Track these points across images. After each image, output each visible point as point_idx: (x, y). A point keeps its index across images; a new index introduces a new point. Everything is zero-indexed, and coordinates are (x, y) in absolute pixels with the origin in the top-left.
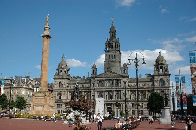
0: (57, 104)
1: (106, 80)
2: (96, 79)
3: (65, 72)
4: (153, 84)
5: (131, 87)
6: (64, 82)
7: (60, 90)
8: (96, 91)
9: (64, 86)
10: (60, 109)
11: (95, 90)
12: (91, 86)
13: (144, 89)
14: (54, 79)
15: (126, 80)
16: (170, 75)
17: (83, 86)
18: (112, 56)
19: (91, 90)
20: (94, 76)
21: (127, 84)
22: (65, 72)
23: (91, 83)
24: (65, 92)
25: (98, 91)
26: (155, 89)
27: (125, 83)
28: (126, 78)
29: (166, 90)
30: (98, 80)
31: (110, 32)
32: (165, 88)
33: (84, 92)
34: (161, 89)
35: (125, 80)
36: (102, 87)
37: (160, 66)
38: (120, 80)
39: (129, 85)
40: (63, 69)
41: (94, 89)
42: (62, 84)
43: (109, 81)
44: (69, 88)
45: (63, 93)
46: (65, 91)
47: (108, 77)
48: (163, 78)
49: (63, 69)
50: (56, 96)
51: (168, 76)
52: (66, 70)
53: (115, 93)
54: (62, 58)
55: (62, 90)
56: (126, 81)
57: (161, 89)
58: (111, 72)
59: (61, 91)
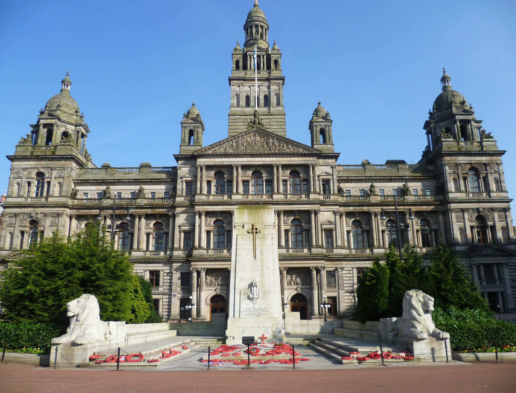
1: (245, 167)
2: (201, 161)
3: (65, 134)
4: (441, 190)
5: (351, 200)
6: (55, 173)
9: (55, 190)
11: (197, 208)
14: (12, 159)
15: (329, 170)
16: (501, 153)
20: (190, 150)
21: (334, 186)
22: (65, 134)
24: (58, 215)
25: (208, 214)
26: (453, 206)
27: (326, 183)
28: (330, 161)
29: (492, 210)
30: (209, 168)
32: (489, 205)
33: (143, 220)
34: (475, 206)
35: (322, 169)
37: (461, 121)
38: (306, 167)
39: (340, 190)
40: (60, 120)
42: (49, 183)
43: (257, 170)
44: (76, 202)
47: (253, 155)
48: (475, 166)
49: (60, 120)
52: (71, 129)
53: (285, 222)
54: (59, 86)
56: (328, 174)
57: (475, 206)
58: (266, 134)
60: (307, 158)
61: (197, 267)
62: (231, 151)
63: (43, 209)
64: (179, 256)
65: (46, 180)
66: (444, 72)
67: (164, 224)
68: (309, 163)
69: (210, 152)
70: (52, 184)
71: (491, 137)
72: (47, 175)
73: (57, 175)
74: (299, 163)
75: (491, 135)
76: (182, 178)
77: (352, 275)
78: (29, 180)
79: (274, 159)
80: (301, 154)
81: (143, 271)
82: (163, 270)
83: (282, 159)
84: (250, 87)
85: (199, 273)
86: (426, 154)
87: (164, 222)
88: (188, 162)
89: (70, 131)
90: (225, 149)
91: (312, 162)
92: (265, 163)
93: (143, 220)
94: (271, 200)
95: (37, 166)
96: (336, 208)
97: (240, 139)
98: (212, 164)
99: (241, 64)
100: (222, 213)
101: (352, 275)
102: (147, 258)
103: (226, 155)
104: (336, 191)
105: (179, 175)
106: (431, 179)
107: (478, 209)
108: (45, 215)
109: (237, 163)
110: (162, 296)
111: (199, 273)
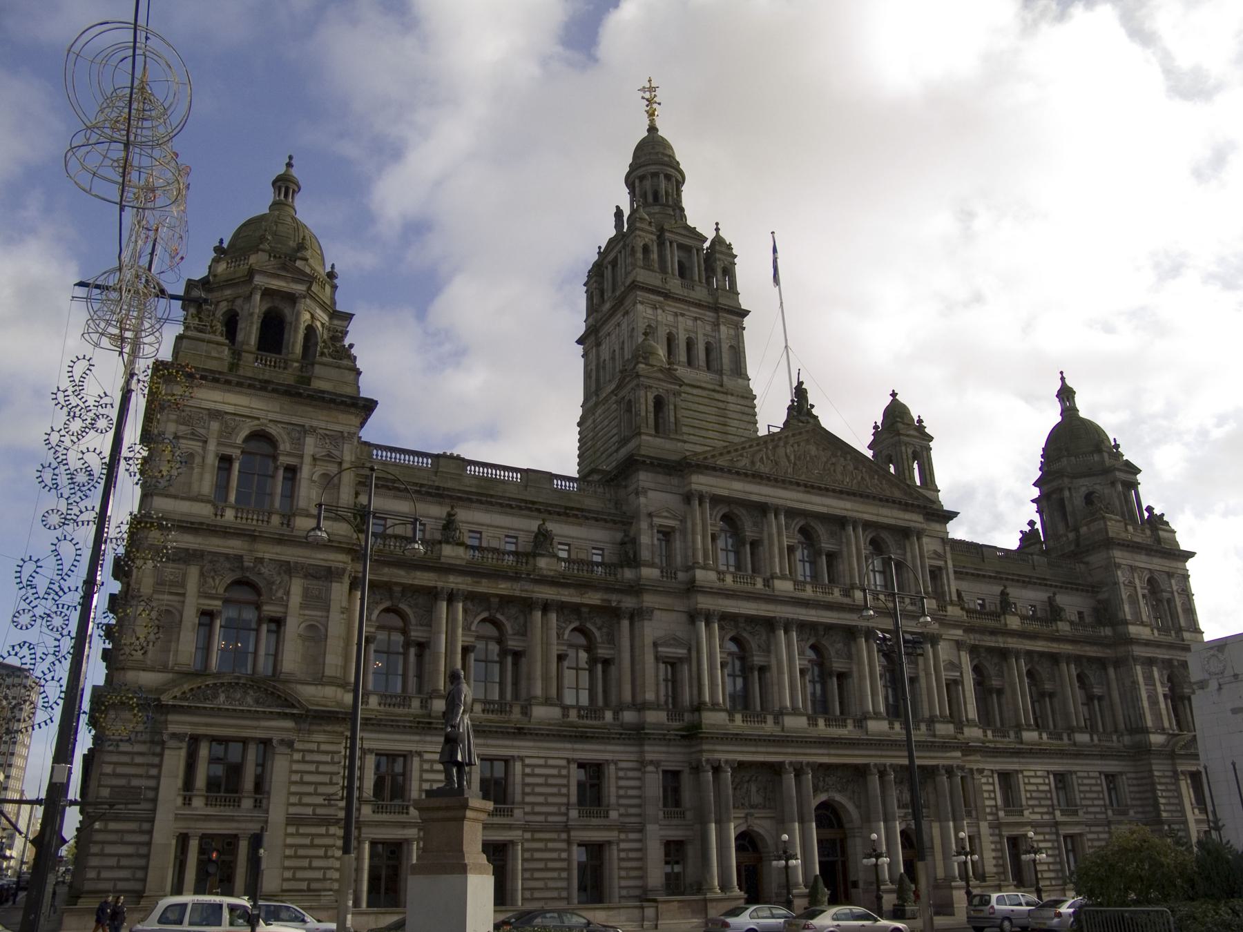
0: (195, 740)
7: (252, 537)
8: (708, 618)
9: (308, 494)
10: (236, 820)
11: (704, 602)
12: (645, 555)
13: (1054, 647)
17: (542, 539)
18: (690, 344)
19: (649, 600)
23: (644, 525)
24: (330, 574)
26: (1138, 651)
27: (936, 573)
28: (937, 527)
31: (633, 181)
33: (553, 617)
36: (759, 584)
41: (691, 588)
45: (297, 588)
46: (338, 559)
47: (809, 488)
48: (1156, 575)
50: (190, 616)
51: (1179, 565)
55: (280, 540)
59: (269, 552)
60: (908, 516)
61: (717, 756)
62: (764, 469)
63: (278, 549)
64: (658, 726)
65: (284, 460)
66: (1063, 379)
67: (597, 634)
68: (912, 524)
69: (720, 462)
70: (305, 472)
71: (1167, 523)
72: (285, 446)
73: (321, 453)
74: (892, 522)
75: (1165, 518)
76: (650, 515)
77: (564, 781)
78: (228, 451)
79: (848, 505)
80: (900, 503)
81: (564, 763)
82: (615, 762)
83: (861, 507)
84: (676, 315)
85: (717, 770)
86: (1028, 538)
87: (599, 629)
88: (661, 478)
89: (319, 324)
90: (753, 463)
91: (917, 525)
92: (831, 511)
93: (553, 617)
94: (846, 600)
95: (256, 413)
96: (958, 633)
97: (781, 444)
98: (725, 493)
99: (655, 256)
100: (751, 620)
101: (564, 781)
102: (572, 725)
103: (757, 477)
104: (955, 598)
105: (644, 511)
106: (1087, 591)
107: (1170, 661)
108: (288, 569)
109: (780, 502)
110: (615, 834)
111: (717, 770)
